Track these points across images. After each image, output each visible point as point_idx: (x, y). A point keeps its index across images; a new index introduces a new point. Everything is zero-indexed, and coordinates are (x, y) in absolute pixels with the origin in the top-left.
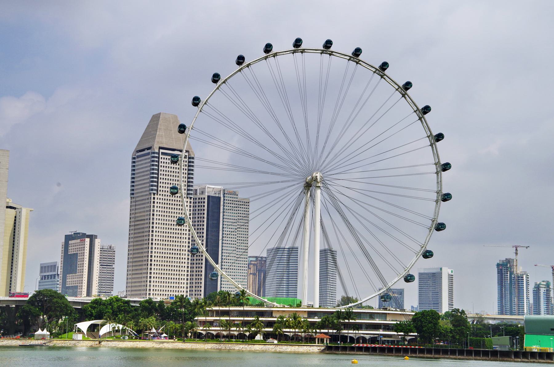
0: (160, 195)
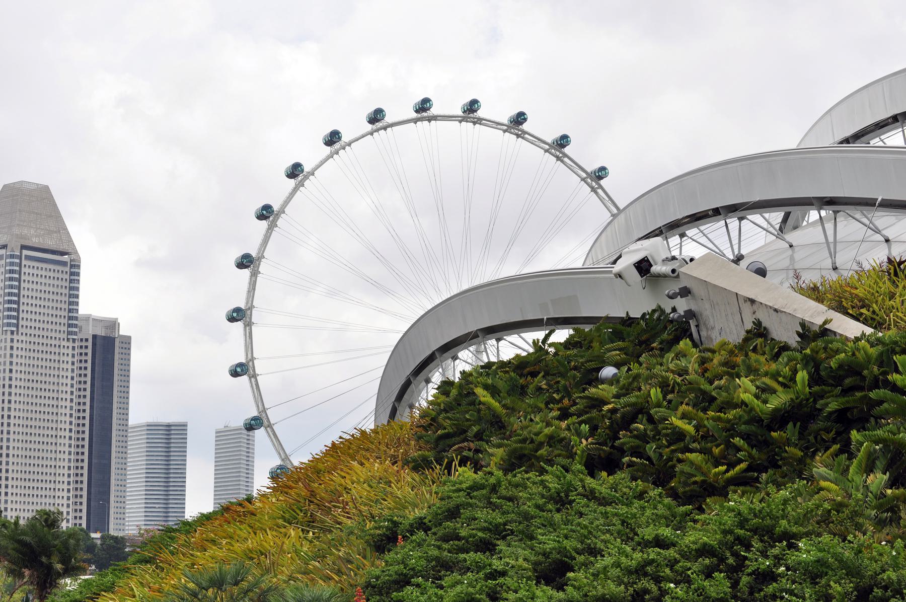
0: (22, 334)
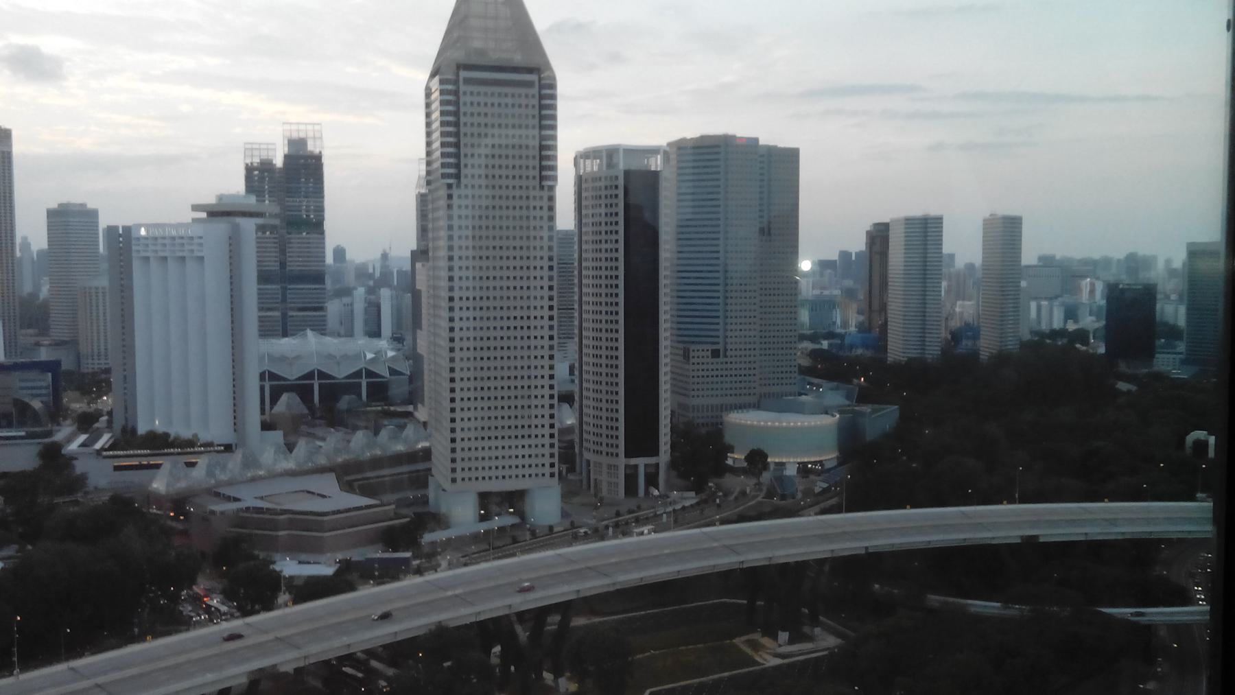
0: (466, 186)
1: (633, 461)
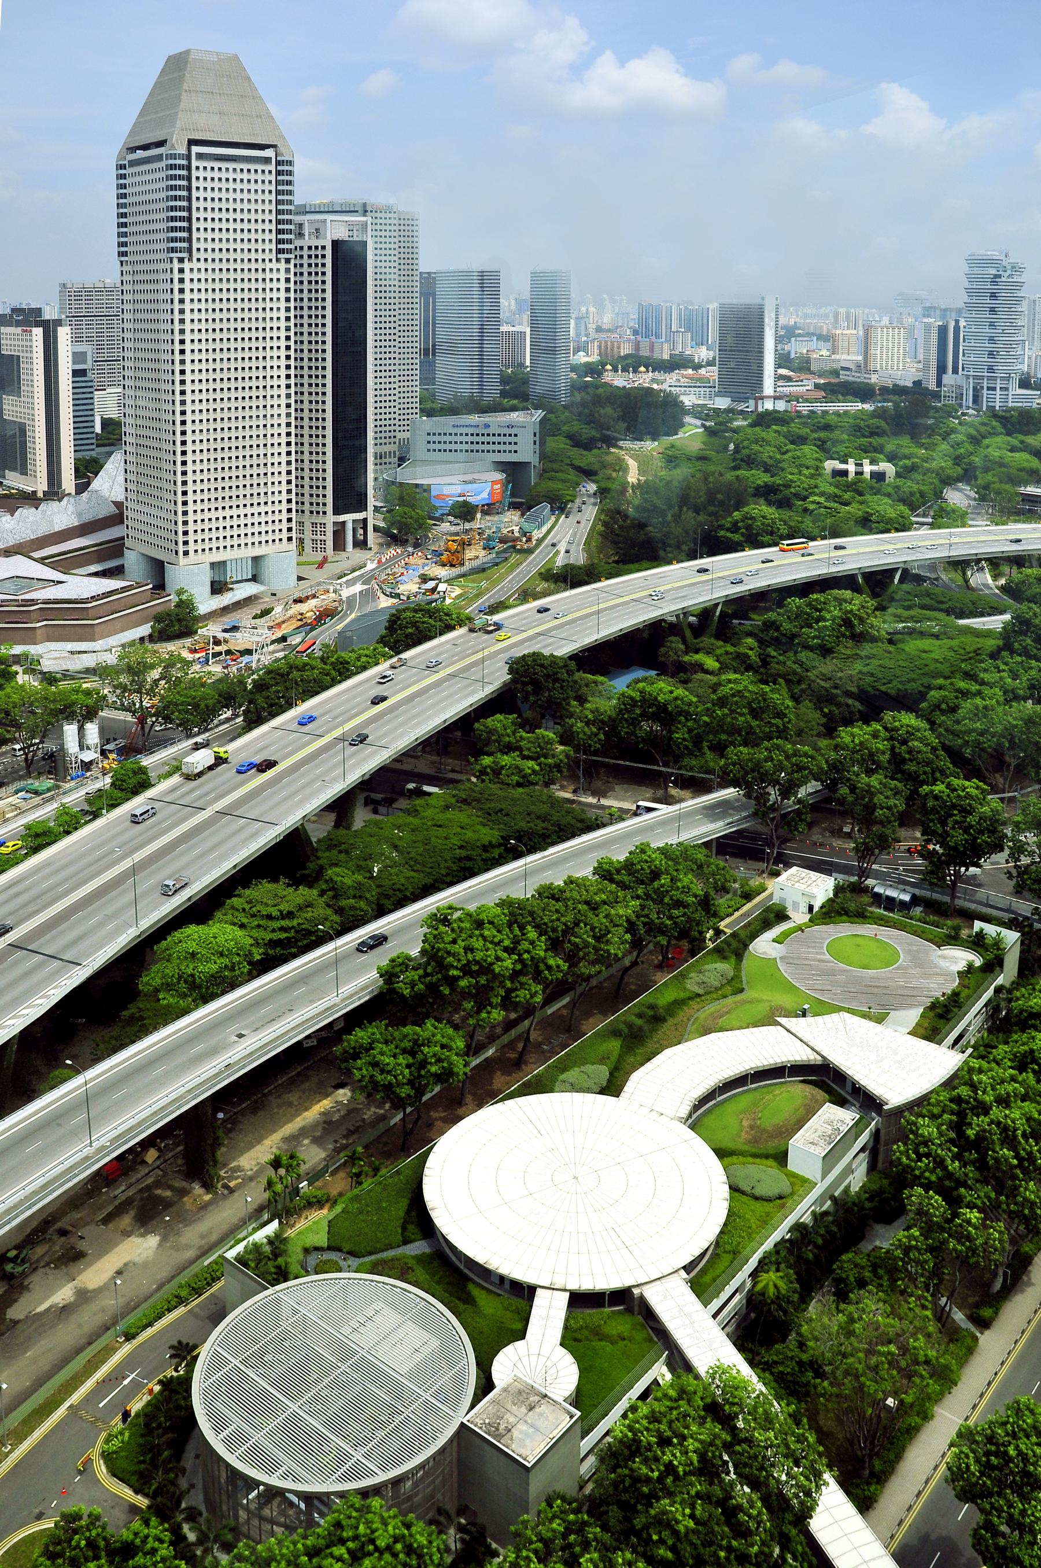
1: (342, 518)
